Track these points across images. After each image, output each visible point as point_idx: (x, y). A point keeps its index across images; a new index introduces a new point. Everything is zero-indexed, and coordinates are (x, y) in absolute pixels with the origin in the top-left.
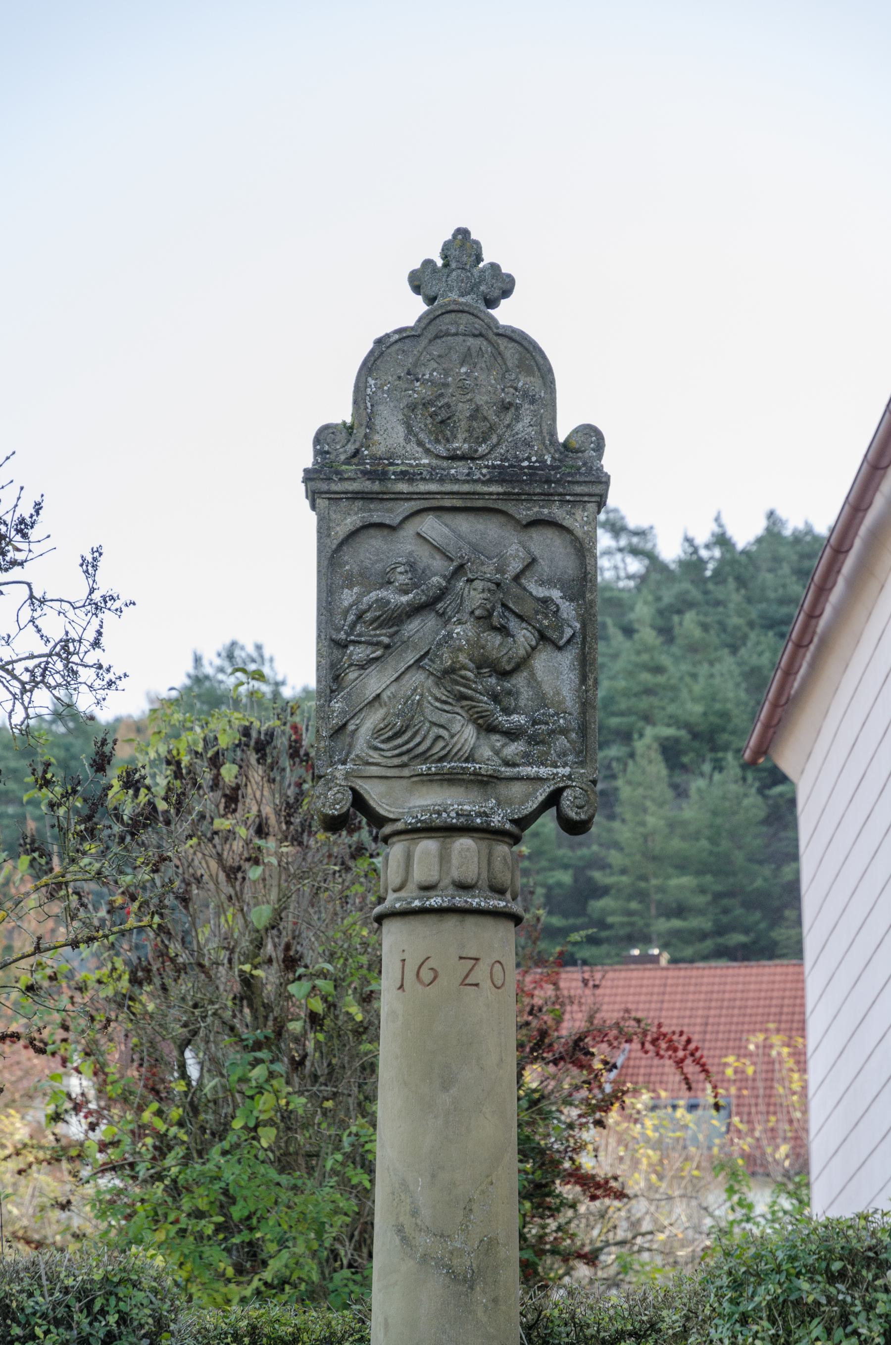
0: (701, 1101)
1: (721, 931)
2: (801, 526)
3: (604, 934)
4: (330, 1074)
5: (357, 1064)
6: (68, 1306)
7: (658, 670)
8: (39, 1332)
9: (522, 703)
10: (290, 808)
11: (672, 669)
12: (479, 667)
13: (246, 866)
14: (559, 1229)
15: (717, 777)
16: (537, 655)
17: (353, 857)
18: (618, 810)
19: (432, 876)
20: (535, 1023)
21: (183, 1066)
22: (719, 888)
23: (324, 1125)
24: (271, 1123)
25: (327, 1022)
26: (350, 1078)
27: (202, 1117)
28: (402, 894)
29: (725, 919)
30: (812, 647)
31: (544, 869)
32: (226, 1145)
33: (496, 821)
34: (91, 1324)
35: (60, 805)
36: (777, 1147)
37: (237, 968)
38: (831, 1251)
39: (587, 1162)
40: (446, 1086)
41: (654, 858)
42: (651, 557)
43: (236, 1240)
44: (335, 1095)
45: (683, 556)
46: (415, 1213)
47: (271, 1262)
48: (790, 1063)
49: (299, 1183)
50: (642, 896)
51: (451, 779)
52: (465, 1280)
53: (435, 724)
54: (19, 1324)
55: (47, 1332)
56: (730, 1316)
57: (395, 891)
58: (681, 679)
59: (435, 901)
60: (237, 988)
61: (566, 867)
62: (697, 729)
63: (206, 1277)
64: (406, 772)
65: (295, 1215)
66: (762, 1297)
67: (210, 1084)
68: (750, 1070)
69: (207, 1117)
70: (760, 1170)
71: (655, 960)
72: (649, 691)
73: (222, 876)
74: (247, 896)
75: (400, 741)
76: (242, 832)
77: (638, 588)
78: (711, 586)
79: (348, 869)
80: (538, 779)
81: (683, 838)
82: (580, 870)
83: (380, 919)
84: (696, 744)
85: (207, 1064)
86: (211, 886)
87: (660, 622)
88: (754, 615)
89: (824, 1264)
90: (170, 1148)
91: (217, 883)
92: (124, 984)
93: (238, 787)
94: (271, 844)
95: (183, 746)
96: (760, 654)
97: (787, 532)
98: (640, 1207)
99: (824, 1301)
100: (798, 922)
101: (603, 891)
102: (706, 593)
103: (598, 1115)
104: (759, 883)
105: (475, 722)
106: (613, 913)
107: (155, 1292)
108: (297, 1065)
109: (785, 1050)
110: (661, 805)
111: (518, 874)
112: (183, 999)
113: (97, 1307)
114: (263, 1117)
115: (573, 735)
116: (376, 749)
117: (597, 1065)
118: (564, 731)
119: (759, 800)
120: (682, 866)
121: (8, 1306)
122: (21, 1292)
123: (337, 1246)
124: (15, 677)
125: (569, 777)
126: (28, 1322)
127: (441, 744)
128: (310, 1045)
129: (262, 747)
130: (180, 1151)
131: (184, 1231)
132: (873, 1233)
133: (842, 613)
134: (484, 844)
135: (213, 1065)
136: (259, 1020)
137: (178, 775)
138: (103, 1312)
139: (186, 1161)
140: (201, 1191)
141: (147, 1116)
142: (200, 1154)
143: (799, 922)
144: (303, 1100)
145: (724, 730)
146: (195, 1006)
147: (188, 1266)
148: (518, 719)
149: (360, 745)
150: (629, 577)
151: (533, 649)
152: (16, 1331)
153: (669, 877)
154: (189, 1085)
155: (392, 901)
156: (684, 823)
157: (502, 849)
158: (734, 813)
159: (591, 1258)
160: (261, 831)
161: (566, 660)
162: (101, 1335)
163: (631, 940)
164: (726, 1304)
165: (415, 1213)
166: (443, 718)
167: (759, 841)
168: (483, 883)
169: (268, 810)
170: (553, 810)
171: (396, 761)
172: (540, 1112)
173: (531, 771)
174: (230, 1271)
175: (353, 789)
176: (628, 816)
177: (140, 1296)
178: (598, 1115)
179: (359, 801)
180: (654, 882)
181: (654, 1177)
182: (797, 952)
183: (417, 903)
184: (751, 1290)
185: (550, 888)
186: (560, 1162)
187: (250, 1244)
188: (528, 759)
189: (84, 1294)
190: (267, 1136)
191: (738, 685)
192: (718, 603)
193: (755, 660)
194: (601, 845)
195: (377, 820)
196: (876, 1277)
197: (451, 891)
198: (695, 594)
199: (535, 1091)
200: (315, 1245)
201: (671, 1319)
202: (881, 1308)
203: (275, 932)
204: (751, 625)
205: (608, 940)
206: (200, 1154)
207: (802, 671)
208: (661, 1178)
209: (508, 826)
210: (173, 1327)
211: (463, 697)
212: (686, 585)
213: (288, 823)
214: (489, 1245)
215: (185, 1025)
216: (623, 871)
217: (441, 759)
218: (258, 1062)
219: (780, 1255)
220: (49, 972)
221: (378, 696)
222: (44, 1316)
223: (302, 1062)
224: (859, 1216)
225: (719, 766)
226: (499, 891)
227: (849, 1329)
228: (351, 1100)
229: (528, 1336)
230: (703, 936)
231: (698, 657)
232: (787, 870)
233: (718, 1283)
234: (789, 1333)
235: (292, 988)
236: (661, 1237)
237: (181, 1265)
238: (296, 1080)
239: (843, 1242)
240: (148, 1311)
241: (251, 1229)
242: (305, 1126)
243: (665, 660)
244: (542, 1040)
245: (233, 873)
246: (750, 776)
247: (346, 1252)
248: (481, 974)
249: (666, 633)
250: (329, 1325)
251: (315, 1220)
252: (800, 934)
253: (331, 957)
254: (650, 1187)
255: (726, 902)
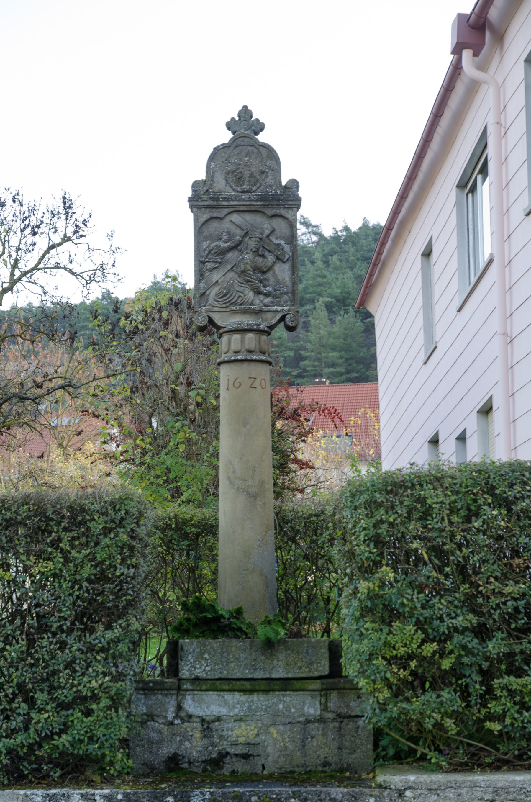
0: (342, 434)
1: (348, 372)
2: (376, 223)
3: (305, 374)
4: (204, 425)
5: (214, 421)
6: (106, 508)
7: (324, 277)
8: (96, 517)
9: (270, 283)
10: (187, 328)
11: (329, 276)
12: (254, 270)
13: (172, 349)
14: (290, 480)
15: (346, 316)
16: (275, 265)
17: (211, 345)
18: (310, 328)
19: (238, 348)
20: (280, 405)
21: (150, 423)
22: (347, 356)
23: (202, 444)
24: (183, 443)
25: (203, 405)
26: (212, 426)
27: (158, 441)
28: (227, 355)
29: (350, 368)
30: (379, 265)
31: (283, 351)
32: (167, 450)
33: (262, 327)
34: (115, 514)
35: (101, 326)
36: (369, 450)
37: (170, 386)
38: (387, 482)
39: (300, 456)
40: (245, 424)
41: (323, 346)
42: (320, 235)
43: (171, 486)
44: (207, 432)
45: (332, 235)
46: (234, 472)
47: (184, 494)
48: (374, 419)
49: (194, 464)
50: (319, 360)
51: (245, 312)
52: (253, 496)
53: (238, 291)
54: (88, 515)
55: (99, 518)
56: (351, 507)
57: (225, 353)
58: (332, 280)
59: (239, 357)
60: (170, 394)
61: (291, 350)
62: (339, 298)
63: (161, 499)
64: (228, 309)
65: (192, 476)
66: (362, 500)
67: (160, 429)
68: (359, 422)
69: (160, 441)
70: (363, 458)
71: (324, 383)
72: (320, 285)
73: (163, 353)
74: (173, 360)
75: (225, 298)
76: (170, 336)
77: (316, 247)
78: (343, 246)
79: (210, 349)
80: (277, 311)
81: (334, 338)
82: (296, 351)
83: (219, 364)
84: (338, 304)
85: (160, 422)
86: (159, 356)
87: (324, 259)
88: (359, 256)
89: (385, 487)
90: (147, 453)
91: (161, 355)
92: (128, 393)
93: (168, 320)
94: (181, 340)
95: (148, 305)
96: (361, 270)
97: (371, 225)
98: (320, 472)
99: (385, 501)
100: (376, 369)
101: (305, 358)
102: (341, 248)
103: (303, 438)
104: (362, 354)
105: (253, 290)
106: (309, 366)
107: (139, 502)
108: (193, 421)
109: (372, 415)
110: (326, 327)
111: (270, 346)
112: (150, 398)
113: (117, 508)
114: (180, 441)
115: (290, 295)
116: (217, 301)
117: (302, 419)
118: (286, 293)
119: (362, 324)
120: (334, 349)
121: (84, 508)
122: (89, 503)
123: (208, 487)
124: (83, 279)
125: (288, 310)
126: (92, 514)
127: (241, 299)
128: (197, 414)
129: (176, 305)
130: (150, 454)
131: (152, 483)
132: (403, 476)
133: (391, 252)
134: (257, 336)
135: (161, 422)
136: (178, 406)
137: (146, 315)
138: (119, 510)
139: (153, 457)
140: (158, 468)
141: (138, 442)
142: (157, 455)
143: (376, 369)
144: (195, 434)
145: (348, 299)
146: (155, 400)
147: (154, 496)
148: (269, 289)
149: (211, 300)
150: (313, 243)
151: (274, 263)
152: (88, 517)
153: (329, 353)
154: (153, 429)
155: (224, 358)
156: (334, 333)
157: (264, 337)
158: (352, 329)
159: (302, 491)
160: (177, 336)
161: (286, 267)
162: (119, 518)
163: (315, 376)
164: (349, 503)
165: (234, 472)
166: (241, 289)
167: (362, 339)
168: (257, 350)
169: (180, 328)
170: (282, 324)
171: (225, 305)
172: (282, 437)
173: (274, 308)
174: (169, 497)
175: (208, 316)
176: (313, 331)
177: (133, 504)
178: (303, 438)
179: (211, 321)
180: (323, 355)
181: (324, 461)
182: (375, 379)
183: (233, 358)
184: (358, 497)
185: (285, 358)
186: (289, 456)
187: (177, 487)
188: (273, 304)
189: (112, 503)
190: (182, 448)
191: (353, 282)
192: (346, 252)
193: (359, 273)
194: (304, 341)
195: (218, 328)
196: (404, 492)
197: (245, 353)
198: (337, 248)
199: (280, 430)
200: (200, 487)
201: (329, 509)
202: (406, 503)
203: (183, 373)
204: (358, 259)
205: (307, 376)
206: (157, 455)
207: (377, 272)
208: (327, 462)
209: (266, 329)
210: (145, 515)
211: (248, 281)
212: (333, 245)
213: (187, 332)
214: (262, 483)
215: (151, 408)
216: (312, 351)
217: (241, 305)
218: (178, 420)
219: (369, 484)
220: (101, 389)
221: (217, 281)
222: (98, 512)
223: (194, 420)
224: (398, 469)
225: (346, 312)
226: (263, 353)
227: (394, 511)
228: (212, 434)
229: (277, 516)
230: (342, 374)
231: (338, 272)
232: (372, 349)
233: (346, 495)
234: (372, 513)
235: (190, 393)
236: (327, 483)
237: (151, 495)
238: (192, 427)
239: (391, 479)
240: (136, 509)
241: (177, 482)
242: (196, 444)
243: (326, 273)
244: (282, 411)
245: (167, 351)
246: (358, 315)
247: (212, 490)
248: (257, 384)
249: (327, 263)
250: (204, 514)
251: (200, 478)
252: (377, 373)
253: (204, 382)
254: (323, 465)
255: (350, 361)
